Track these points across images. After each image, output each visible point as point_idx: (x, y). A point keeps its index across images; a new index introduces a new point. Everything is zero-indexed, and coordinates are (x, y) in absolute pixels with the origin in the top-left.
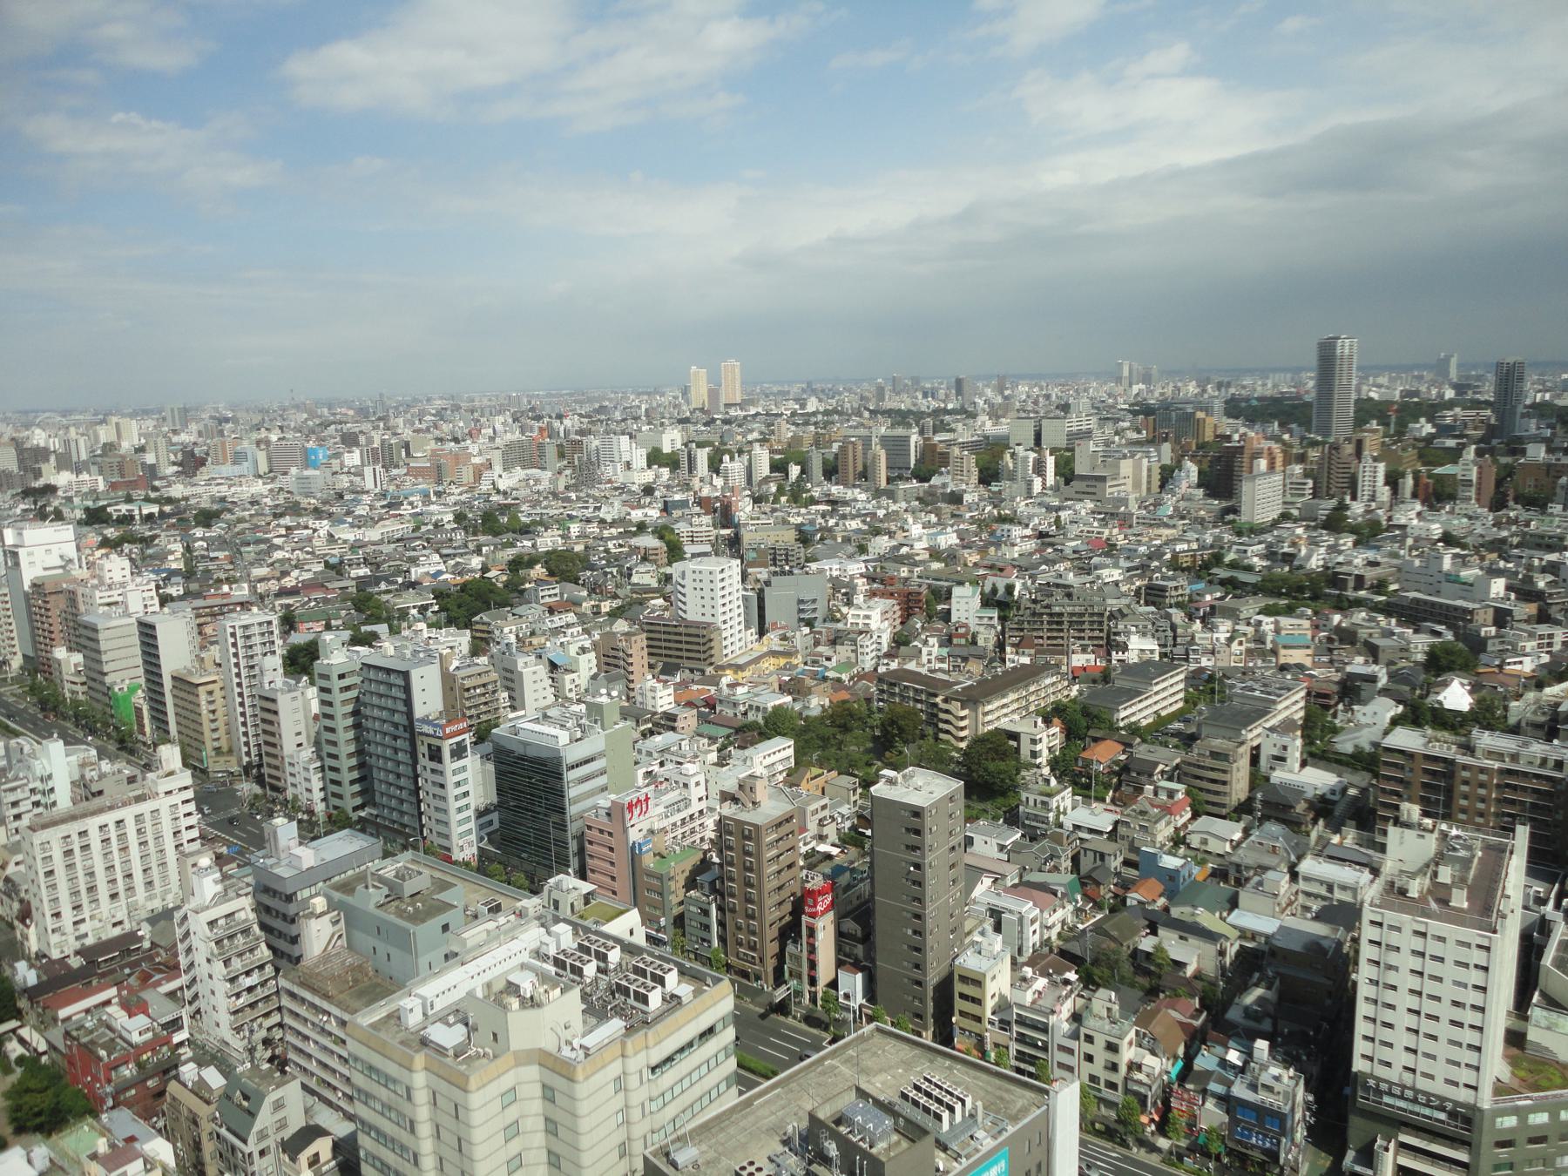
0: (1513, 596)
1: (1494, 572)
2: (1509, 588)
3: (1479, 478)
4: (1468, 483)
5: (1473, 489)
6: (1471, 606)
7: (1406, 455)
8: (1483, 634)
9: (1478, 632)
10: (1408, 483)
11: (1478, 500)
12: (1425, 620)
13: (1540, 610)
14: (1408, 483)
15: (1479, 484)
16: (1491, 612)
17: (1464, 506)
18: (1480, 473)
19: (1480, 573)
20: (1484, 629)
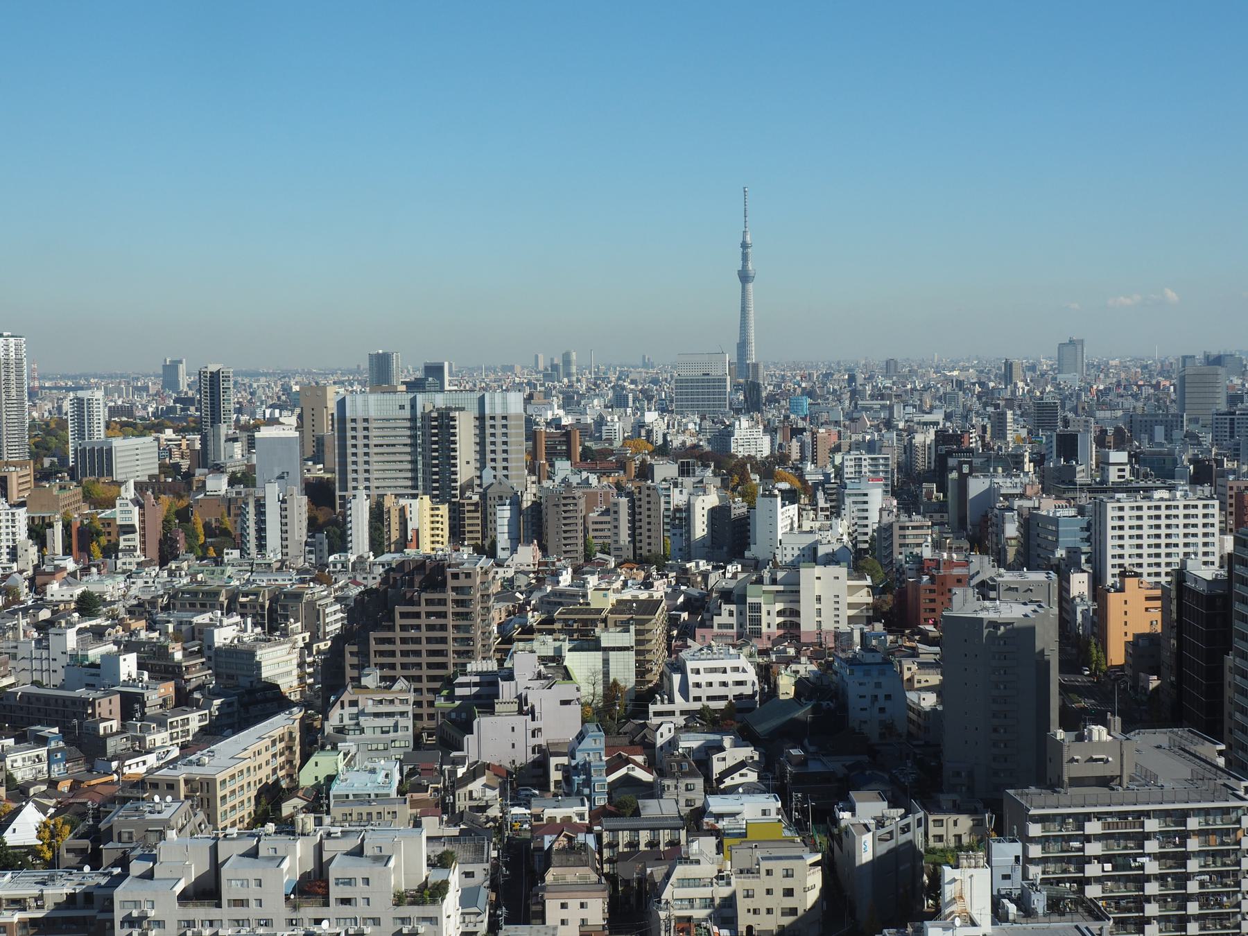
0: (146, 675)
1: (129, 647)
2: (141, 666)
3: (142, 522)
4: (129, 529)
5: (137, 536)
6: (91, 695)
7: (66, 493)
8: (102, 732)
9: (97, 729)
10: (56, 536)
11: (144, 550)
12: (39, 723)
13: (178, 690)
14: (56, 536)
15: (143, 529)
16: (116, 699)
17: (128, 560)
18: (142, 515)
19: (115, 648)
20: (102, 726)
